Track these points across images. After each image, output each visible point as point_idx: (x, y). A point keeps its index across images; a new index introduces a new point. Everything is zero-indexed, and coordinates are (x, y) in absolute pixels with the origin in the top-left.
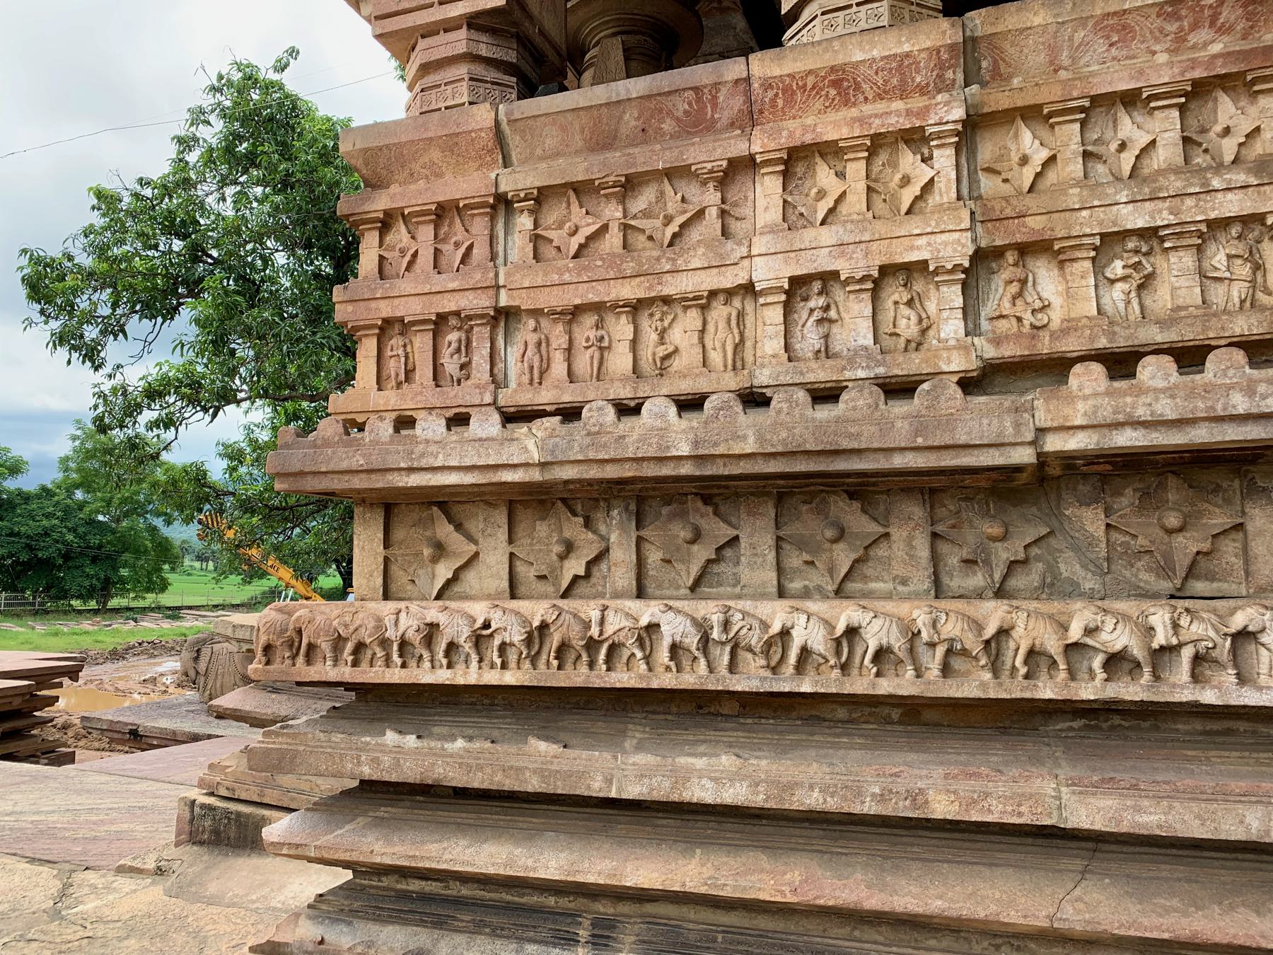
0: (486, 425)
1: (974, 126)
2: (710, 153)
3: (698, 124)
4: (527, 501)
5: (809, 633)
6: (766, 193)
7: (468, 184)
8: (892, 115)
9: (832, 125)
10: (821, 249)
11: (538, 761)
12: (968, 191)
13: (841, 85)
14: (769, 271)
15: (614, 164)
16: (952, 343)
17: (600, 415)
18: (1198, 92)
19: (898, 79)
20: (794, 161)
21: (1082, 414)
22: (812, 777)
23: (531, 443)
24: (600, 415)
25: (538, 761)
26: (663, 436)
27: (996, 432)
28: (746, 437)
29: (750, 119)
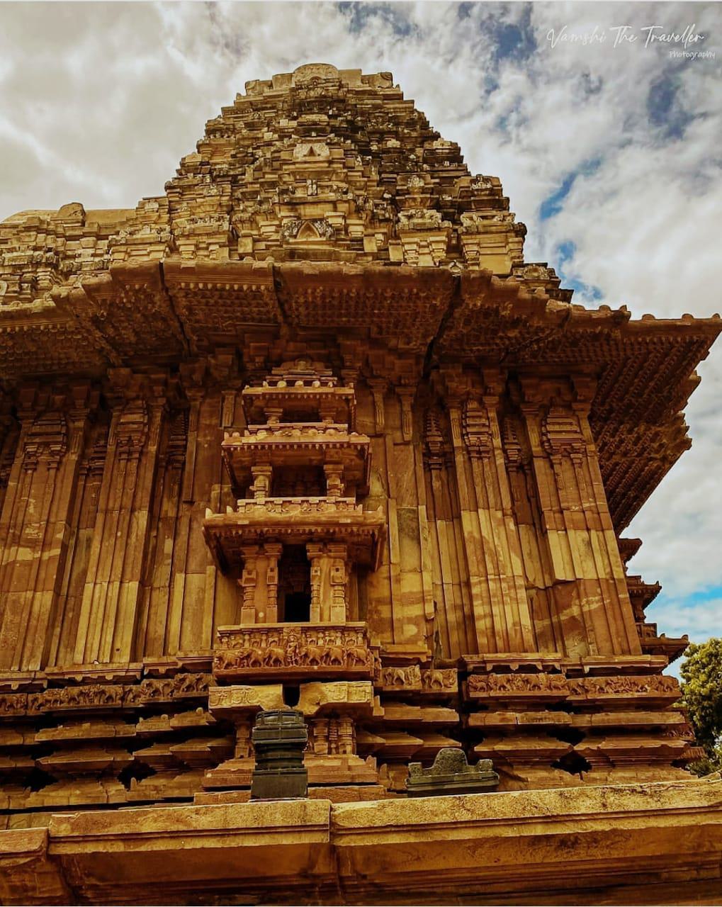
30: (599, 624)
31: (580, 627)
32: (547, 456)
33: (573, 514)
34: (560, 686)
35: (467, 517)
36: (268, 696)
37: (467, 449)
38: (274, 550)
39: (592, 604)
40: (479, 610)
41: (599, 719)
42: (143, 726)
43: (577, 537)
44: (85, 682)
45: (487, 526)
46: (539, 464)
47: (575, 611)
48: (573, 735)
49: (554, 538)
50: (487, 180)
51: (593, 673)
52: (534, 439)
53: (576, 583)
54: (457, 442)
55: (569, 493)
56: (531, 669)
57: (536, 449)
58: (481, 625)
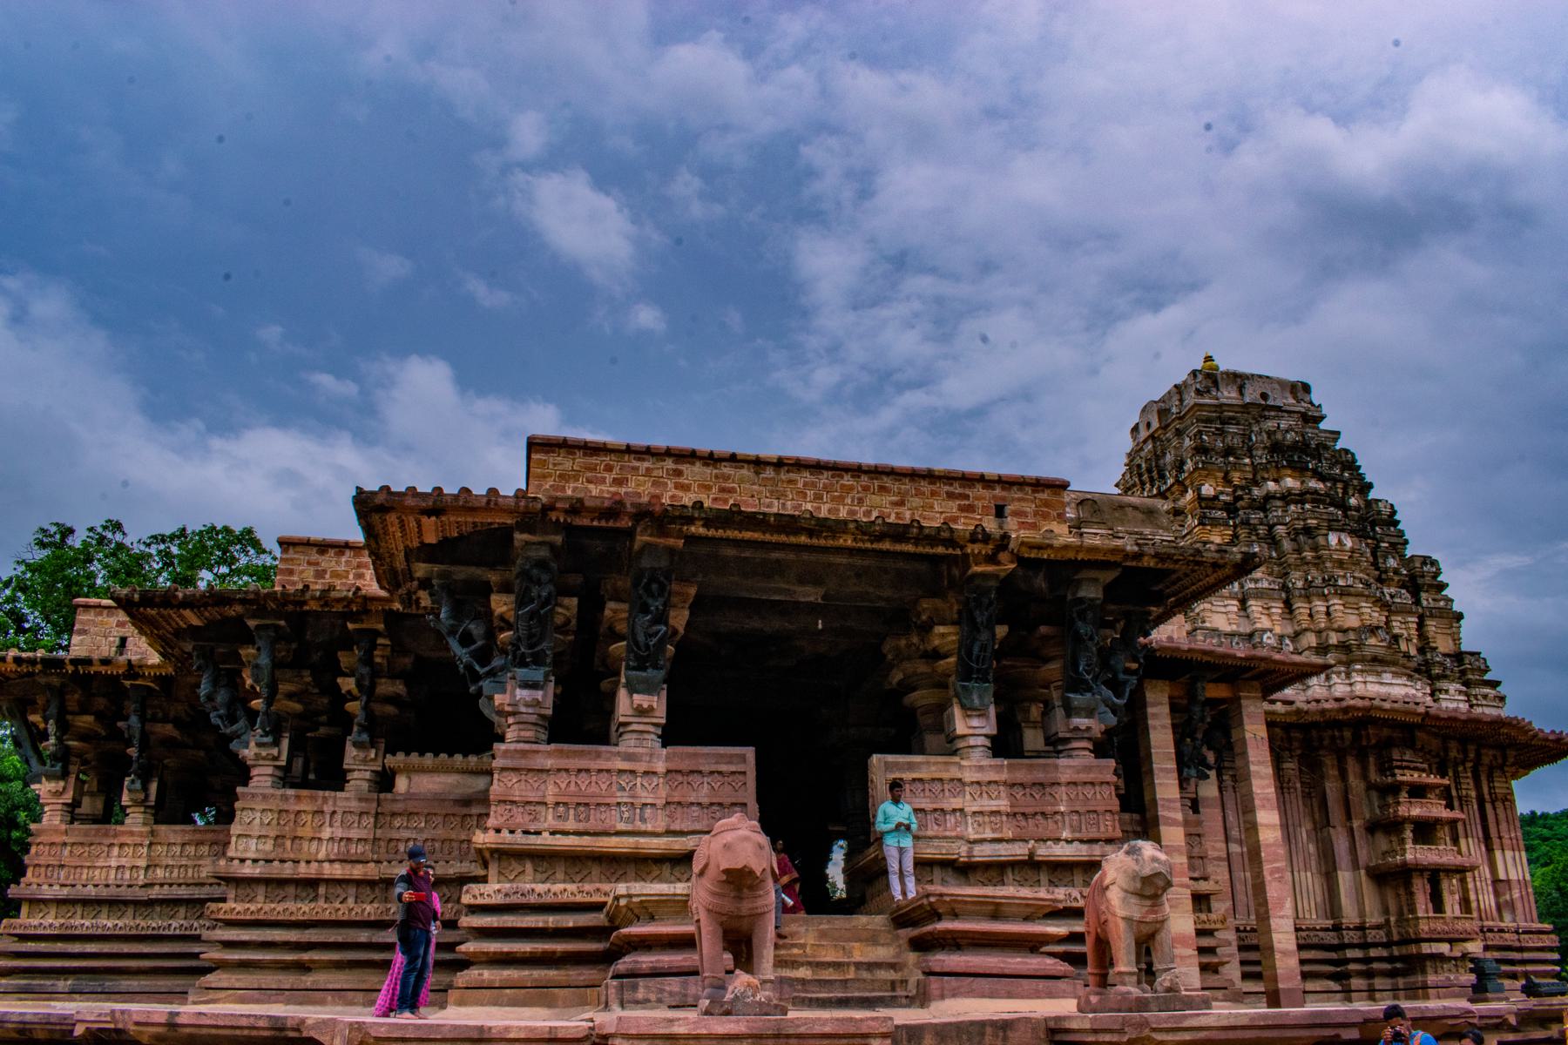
0: (56, 887)
1: (151, 844)
2: (107, 841)
3: (106, 835)
4: (60, 902)
5: (110, 924)
6: (116, 850)
7: (59, 839)
8: (138, 840)
9: (128, 840)
10: (123, 861)
11: (59, 947)
12: (149, 855)
13: (132, 833)
14: (114, 863)
15: (89, 839)
16: (141, 879)
17: (79, 887)
18: (184, 845)
19: (141, 834)
20: (121, 845)
21: (155, 893)
22: (106, 948)
23: (65, 891)
24: (79, 887)
25: (59, 947)
26: (91, 891)
27: (143, 895)
28: (104, 893)
29: (115, 836)
30: (1519, 905)
31: (1511, 905)
32: (1493, 802)
33: (1506, 842)
34: (1510, 938)
35: (1462, 842)
36: (1444, 948)
37: (1460, 798)
38: (1426, 874)
39: (1516, 895)
40: (1472, 897)
41: (1526, 955)
42: (1350, 954)
43: (1509, 854)
44: (1308, 929)
45: (1471, 850)
46: (1488, 807)
47: (1508, 897)
48: (1512, 962)
49: (1498, 854)
50: (1434, 563)
51: (1525, 932)
52: (1486, 790)
53: (1508, 881)
54: (1454, 793)
55: (1503, 826)
56: (1501, 931)
57: (1487, 797)
58: (1474, 905)
